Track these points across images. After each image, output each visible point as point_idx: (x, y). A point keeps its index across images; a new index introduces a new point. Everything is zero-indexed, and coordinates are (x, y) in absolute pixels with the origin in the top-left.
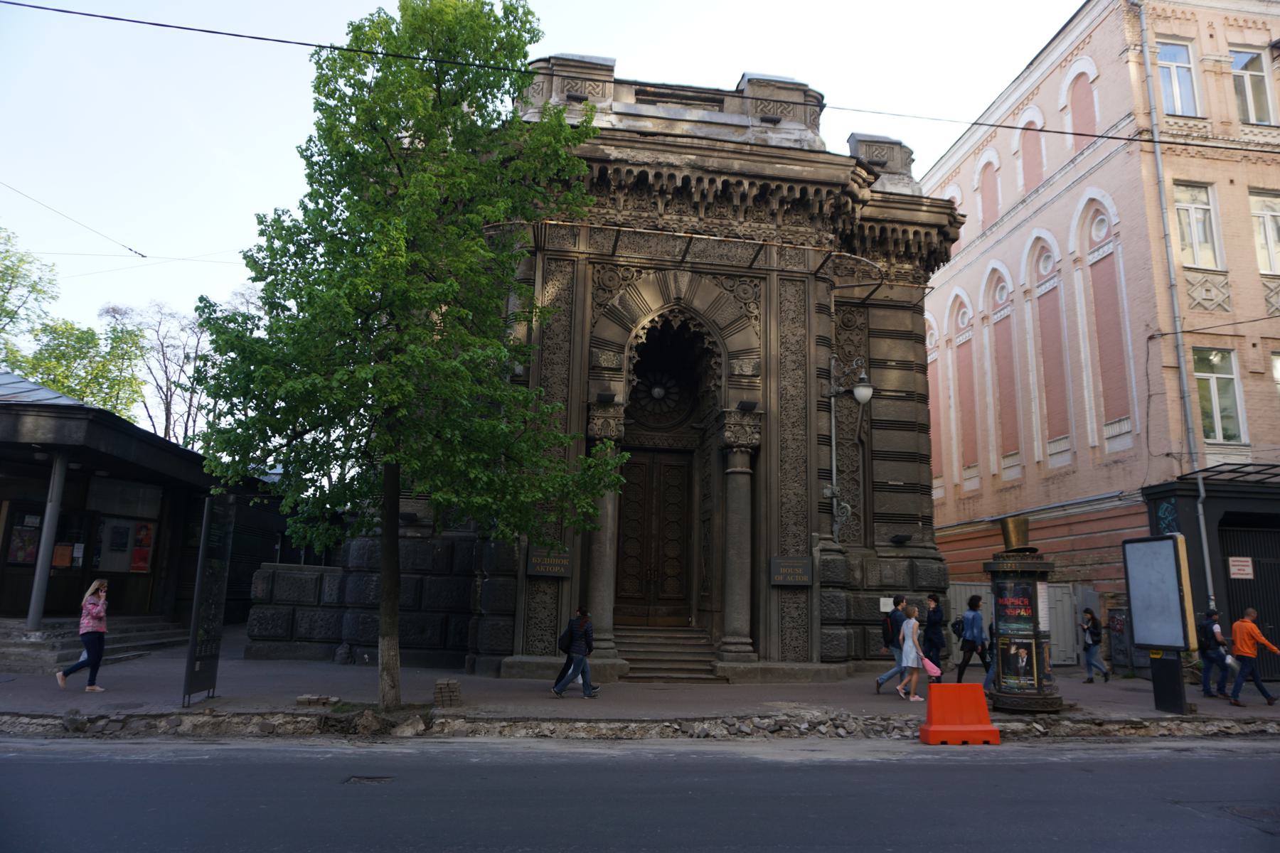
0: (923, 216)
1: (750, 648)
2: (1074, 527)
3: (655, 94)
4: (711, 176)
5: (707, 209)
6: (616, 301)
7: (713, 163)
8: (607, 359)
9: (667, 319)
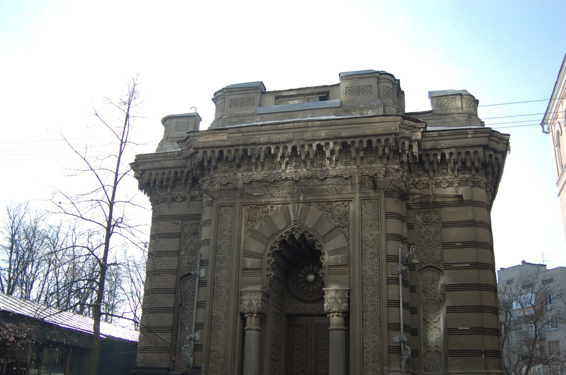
0: (470, 141)
4: (309, 143)
5: (312, 162)
7: (308, 136)
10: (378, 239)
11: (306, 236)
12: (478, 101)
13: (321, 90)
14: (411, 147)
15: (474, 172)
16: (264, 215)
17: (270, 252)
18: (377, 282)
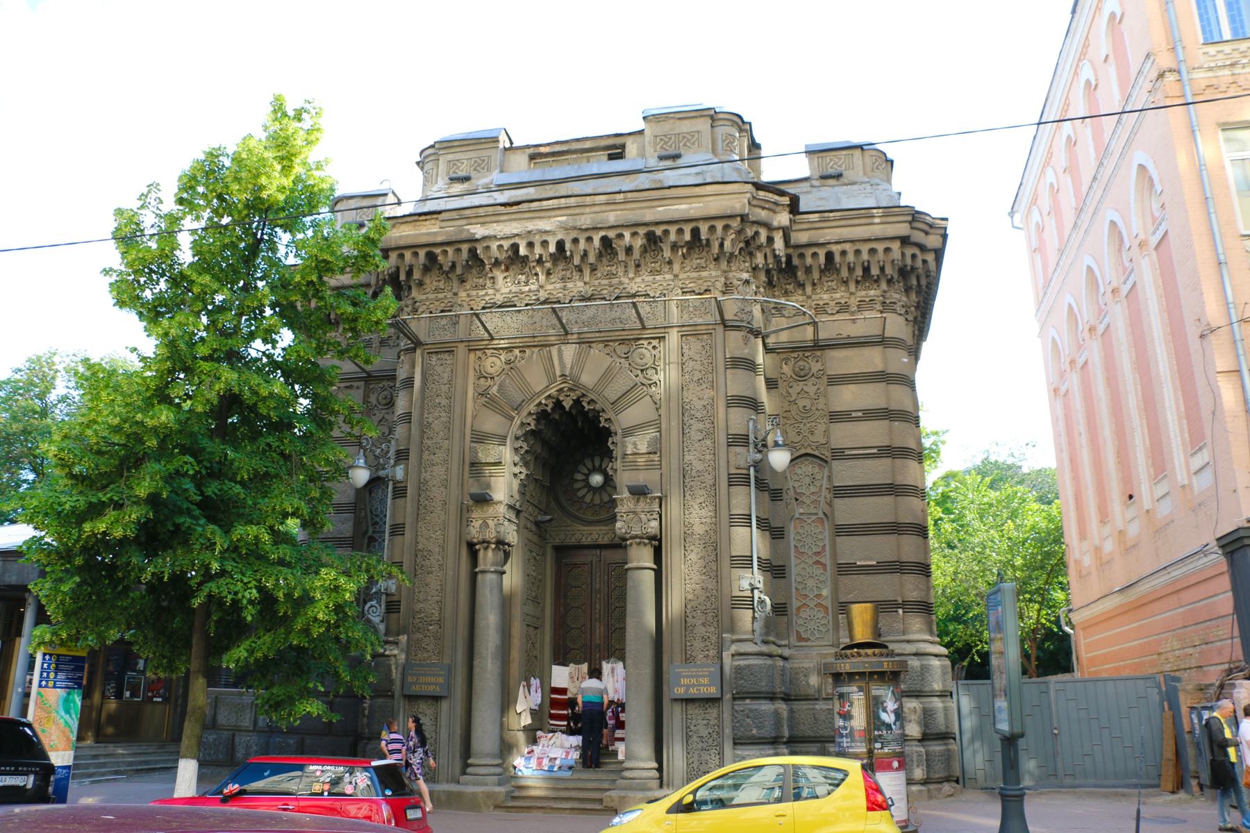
0: (877, 230)
2: (1183, 595)
3: (553, 154)
4: (587, 234)
5: (594, 269)
6: (494, 390)
7: (585, 221)
9: (558, 400)
10: (712, 406)
12: (892, 162)
14: (770, 240)
15: (884, 286)
17: (520, 433)
18: (711, 482)
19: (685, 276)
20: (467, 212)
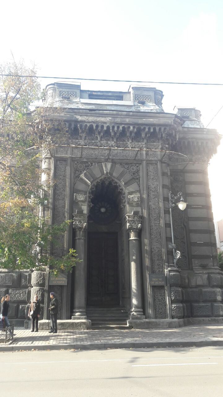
1: (142, 313)
4: (118, 125)
5: (117, 139)
7: (118, 120)
8: (81, 197)
11: (113, 183)
12: (201, 115)
13: (118, 94)
14: (176, 135)
16: (87, 168)
19: (149, 143)
20: (76, 110)
